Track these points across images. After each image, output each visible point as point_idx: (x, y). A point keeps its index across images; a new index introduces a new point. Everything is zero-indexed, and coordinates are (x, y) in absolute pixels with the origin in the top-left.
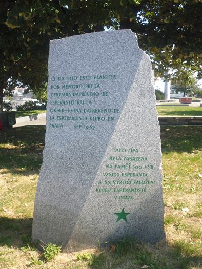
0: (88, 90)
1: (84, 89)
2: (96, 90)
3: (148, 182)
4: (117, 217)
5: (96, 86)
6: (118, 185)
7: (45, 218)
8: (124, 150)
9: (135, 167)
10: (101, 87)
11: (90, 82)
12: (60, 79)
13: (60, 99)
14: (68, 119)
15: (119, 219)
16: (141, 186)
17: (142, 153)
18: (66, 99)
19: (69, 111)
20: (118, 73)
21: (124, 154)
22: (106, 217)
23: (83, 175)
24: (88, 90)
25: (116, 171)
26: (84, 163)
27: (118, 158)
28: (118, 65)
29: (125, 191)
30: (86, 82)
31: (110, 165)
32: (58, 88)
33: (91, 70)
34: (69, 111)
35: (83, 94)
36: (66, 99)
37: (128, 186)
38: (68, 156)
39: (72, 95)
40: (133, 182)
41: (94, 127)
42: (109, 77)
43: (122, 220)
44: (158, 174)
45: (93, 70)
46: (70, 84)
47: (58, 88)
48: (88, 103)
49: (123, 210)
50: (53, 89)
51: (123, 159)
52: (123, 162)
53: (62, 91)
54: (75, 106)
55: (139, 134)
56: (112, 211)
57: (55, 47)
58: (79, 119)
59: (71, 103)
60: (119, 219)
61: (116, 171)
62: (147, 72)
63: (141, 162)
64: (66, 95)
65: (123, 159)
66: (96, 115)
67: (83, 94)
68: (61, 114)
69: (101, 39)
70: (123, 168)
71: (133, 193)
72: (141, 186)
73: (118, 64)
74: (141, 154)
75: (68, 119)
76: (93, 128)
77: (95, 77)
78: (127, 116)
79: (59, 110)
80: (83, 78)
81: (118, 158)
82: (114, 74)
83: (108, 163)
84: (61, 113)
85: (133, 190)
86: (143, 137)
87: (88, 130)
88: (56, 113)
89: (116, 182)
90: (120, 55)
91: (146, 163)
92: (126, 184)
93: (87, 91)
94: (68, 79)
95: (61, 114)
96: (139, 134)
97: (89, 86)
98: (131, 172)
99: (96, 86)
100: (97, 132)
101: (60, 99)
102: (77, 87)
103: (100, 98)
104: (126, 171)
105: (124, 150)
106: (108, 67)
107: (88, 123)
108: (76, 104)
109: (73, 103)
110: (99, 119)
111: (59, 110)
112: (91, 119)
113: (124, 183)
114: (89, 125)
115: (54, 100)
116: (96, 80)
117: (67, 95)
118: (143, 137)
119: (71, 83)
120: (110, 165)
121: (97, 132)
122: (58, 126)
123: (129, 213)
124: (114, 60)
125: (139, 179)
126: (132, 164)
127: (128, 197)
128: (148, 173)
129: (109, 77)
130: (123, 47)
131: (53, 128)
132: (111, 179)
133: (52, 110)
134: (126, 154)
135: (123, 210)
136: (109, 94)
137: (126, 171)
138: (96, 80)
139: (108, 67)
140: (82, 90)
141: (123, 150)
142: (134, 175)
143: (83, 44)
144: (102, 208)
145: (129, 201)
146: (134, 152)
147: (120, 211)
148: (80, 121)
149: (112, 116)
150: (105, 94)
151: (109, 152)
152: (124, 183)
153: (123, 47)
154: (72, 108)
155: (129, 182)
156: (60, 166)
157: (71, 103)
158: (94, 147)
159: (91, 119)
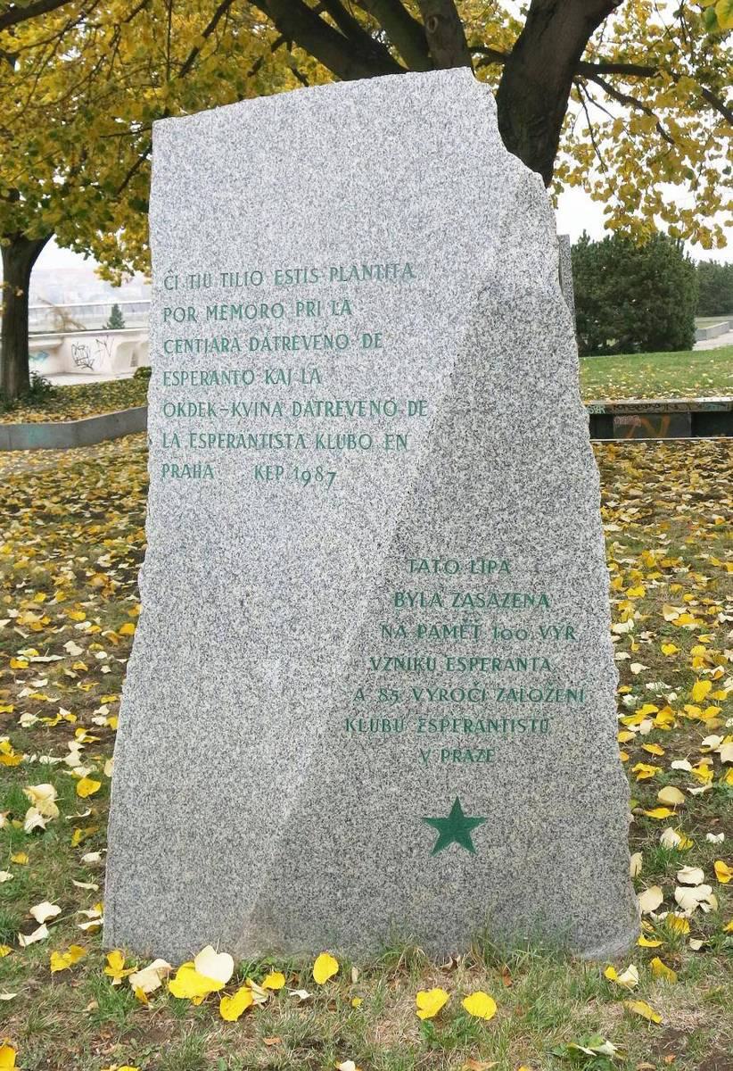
0: (307, 326)
1: (291, 321)
2: (335, 326)
3: (554, 692)
4: (433, 834)
5: (339, 309)
7: (155, 838)
8: (452, 567)
9: (500, 634)
10: (356, 312)
11: (313, 290)
12: (195, 282)
13: (201, 361)
14: (231, 442)
15: (441, 844)
16: (527, 710)
17: (528, 577)
18: (223, 362)
19: (235, 410)
20: (422, 251)
21: (454, 581)
22: (390, 833)
23: (294, 666)
24: (307, 326)
25: (424, 649)
26: (295, 619)
27: (429, 596)
28: (421, 220)
29: (461, 729)
30: (300, 294)
31: (396, 627)
32: (192, 317)
33: (316, 244)
34: (235, 410)
35: (287, 343)
38: (237, 591)
39: (245, 349)
40: (493, 694)
41: (334, 474)
42: (387, 271)
43: (454, 845)
44: (597, 659)
45: (323, 242)
46: (235, 299)
47: (192, 317)
48: (308, 379)
49: (457, 804)
50: (173, 322)
51: (448, 601)
53: (209, 330)
54: (259, 389)
55: (511, 504)
56: (413, 809)
57: (174, 147)
58: (274, 442)
59: (242, 378)
60: (441, 844)
61: (424, 649)
62: (536, 246)
63: (526, 613)
64: (222, 345)
65: (448, 601)
66: (338, 426)
67: (287, 343)
68: (206, 427)
69: (354, 111)
70: (452, 640)
71: (495, 736)
72: (527, 710)
73: (420, 217)
75: (231, 442)
76: (328, 477)
77: (334, 272)
78: (460, 428)
79: (196, 409)
80: (287, 278)
81: (429, 596)
82: (406, 259)
83: (388, 619)
84: (205, 421)
85: (496, 728)
86: (530, 511)
87: (309, 489)
88: (185, 421)
89: (426, 695)
90: (430, 180)
91: (549, 620)
92: (466, 703)
93: (303, 331)
95: (206, 427)
96: (511, 504)
97: (310, 308)
98: (484, 652)
99: (339, 309)
100: (342, 493)
101: (201, 361)
102: (264, 314)
103: (353, 357)
104: (465, 648)
105: (452, 567)
106: (380, 231)
107: (311, 460)
108: (260, 382)
109: (248, 377)
110: (350, 440)
111: (196, 409)
112: (319, 442)
113: (458, 697)
114: (312, 465)
115: (175, 366)
116: (336, 284)
117: (225, 348)
118: (530, 511)
120: (396, 627)
121: (342, 493)
122: (194, 471)
123: (482, 820)
124: (406, 201)
125: (519, 680)
126: (487, 622)
127: (476, 753)
128: (556, 659)
129: (387, 271)
130: (440, 144)
131: (174, 480)
132: (408, 681)
133: (169, 410)
135: (457, 804)
136: (385, 342)
137: (465, 648)
138: (336, 284)
139: (380, 231)
140: (281, 327)
141: (442, 565)
142: (496, 666)
143: (285, 134)
144: (374, 798)
145: (478, 769)
146: (495, 575)
147: (444, 810)
148: (280, 453)
149: (400, 429)
150: (371, 341)
152: (458, 697)
153: (440, 144)
154: (248, 401)
156: (208, 632)
157: (242, 378)
158: (333, 555)
159: (319, 442)
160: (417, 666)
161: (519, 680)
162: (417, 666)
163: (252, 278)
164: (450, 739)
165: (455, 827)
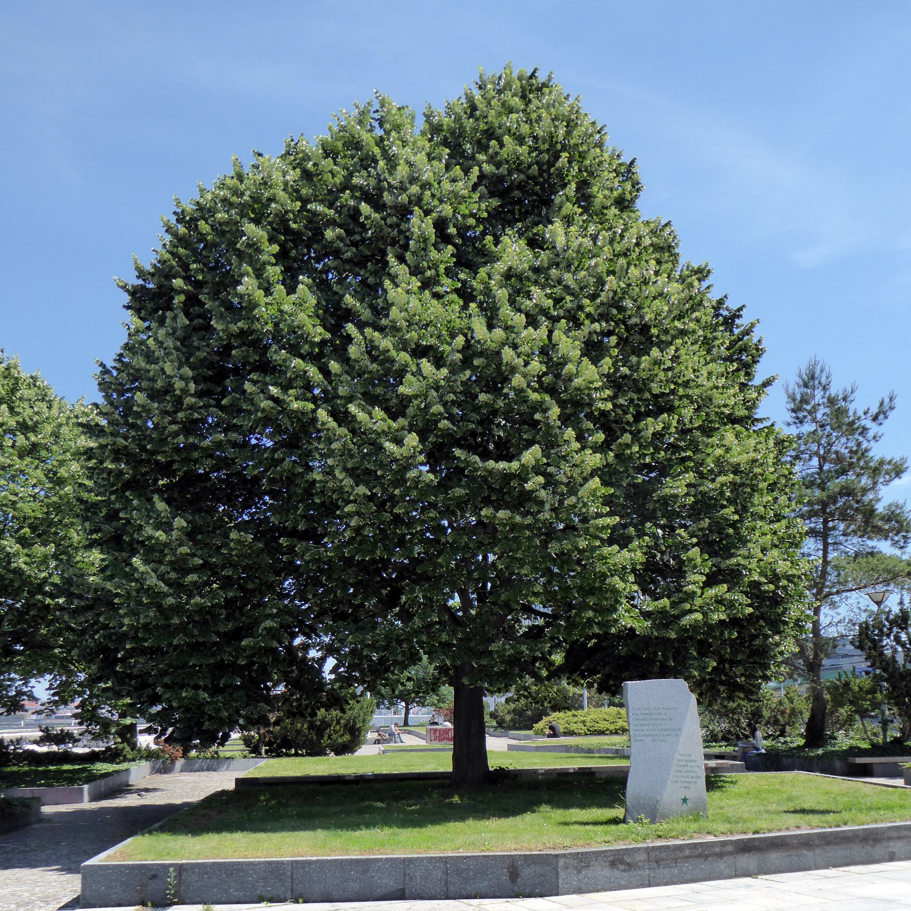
0: (659, 717)
6: (683, 779)
13: (640, 722)
14: (647, 736)
16: (694, 780)
18: (644, 723)
24: (659, 717)
25: (681, 769)
35: (656, 719)
36: (644, 723)
37: (687, 780)
52: (684, 763)
53: (641, 717)
61: (681, 769)
66: (666, 733)
67: (656, 719)
72: (694, 780)
74: (693, 758)
75: (647, 736)
80: (655, 709)
94: (645, 709)
119: (647, 712)
125: (693, 775)
132: (679, 774)
134: (686, 758)
137: (686, 769)
141: (684, 755)
151: (677, 756)
155: (687, 777)
160: (680, 771)
161: (693, 775)
162: (680, 771)
163: (649, 709)
164: (685, 785)
165: (685, 800)
